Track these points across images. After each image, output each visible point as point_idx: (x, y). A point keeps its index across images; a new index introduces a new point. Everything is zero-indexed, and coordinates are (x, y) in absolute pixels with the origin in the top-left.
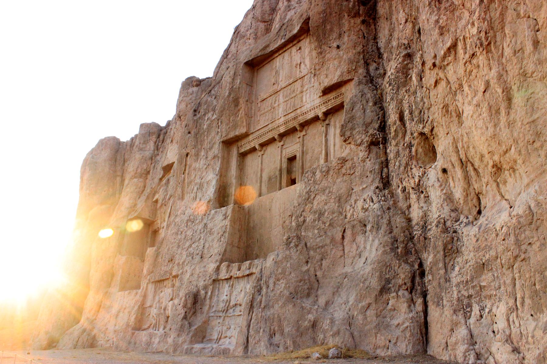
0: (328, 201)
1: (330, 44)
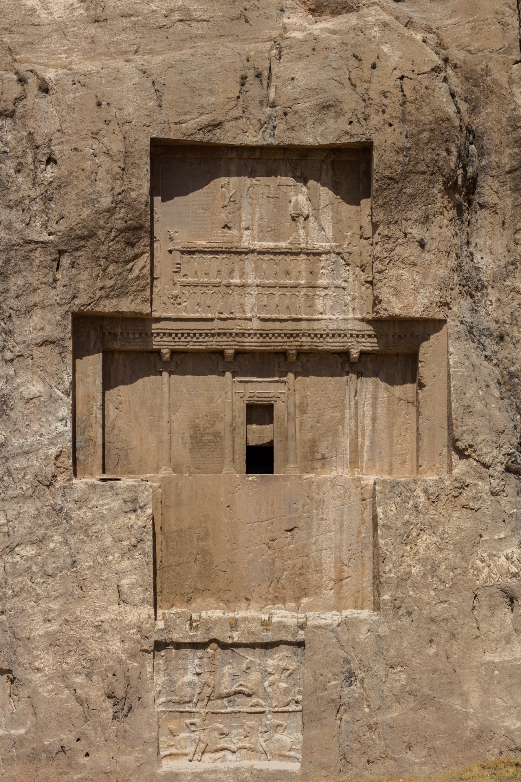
0: (443, 546)
1: (406, 227)
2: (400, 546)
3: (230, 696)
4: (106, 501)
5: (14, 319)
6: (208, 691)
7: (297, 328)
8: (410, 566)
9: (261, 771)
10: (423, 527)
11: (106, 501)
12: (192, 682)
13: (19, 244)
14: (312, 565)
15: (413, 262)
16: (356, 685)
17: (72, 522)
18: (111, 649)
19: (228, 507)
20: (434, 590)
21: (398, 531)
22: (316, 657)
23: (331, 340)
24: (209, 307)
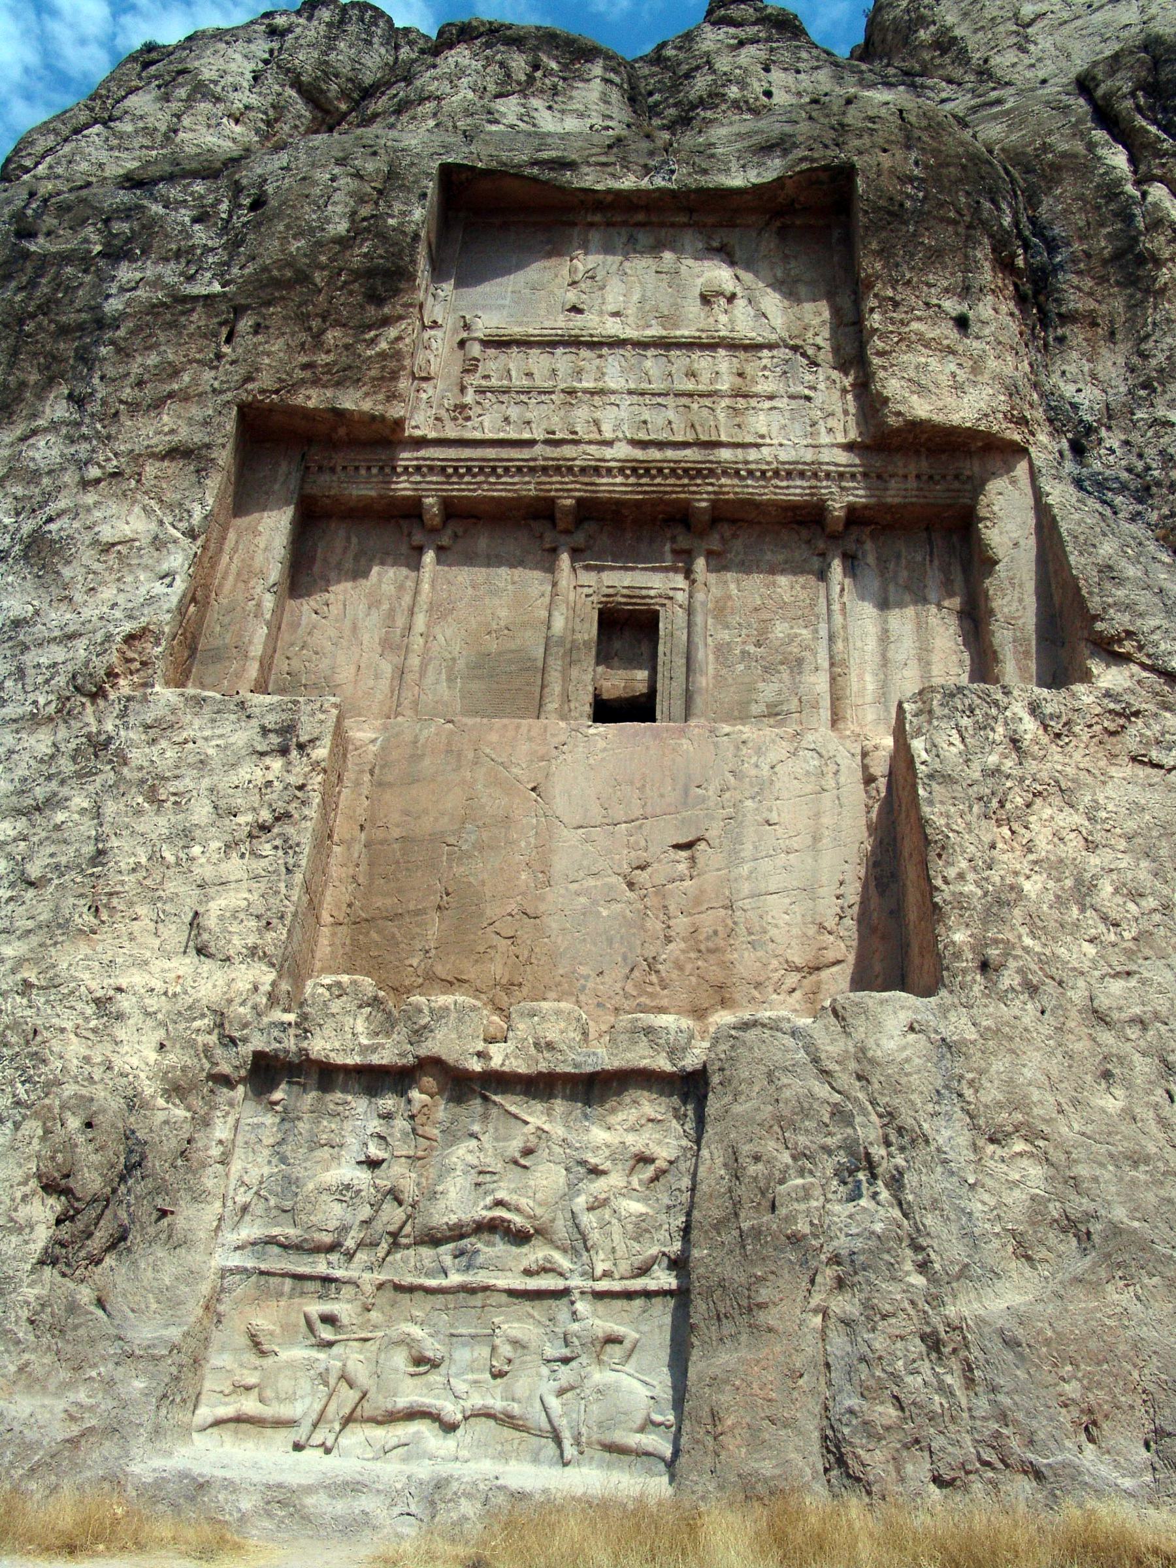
0: (1098, 837)
2: (984, 822)
3: (462, 1237)
4: (218, 732)
5: (123, 418)
6: (393, 1215)
7: (711, 458)
8: (1016, 874)
9: (519, 1496)
10: (1040, 788)
11: (218, 732)
12: (348, 1187)
13: (163, 304)
14: (741, 930)
15: (948, 347)
16: (875, 1195)
17: (125, 770)
18: (117, 1063)
19: (533, 789)
20: (1091, 941)
21: (975, 788)
22: (737, 1109)
23: (784, 484)
24: (529, 423)
